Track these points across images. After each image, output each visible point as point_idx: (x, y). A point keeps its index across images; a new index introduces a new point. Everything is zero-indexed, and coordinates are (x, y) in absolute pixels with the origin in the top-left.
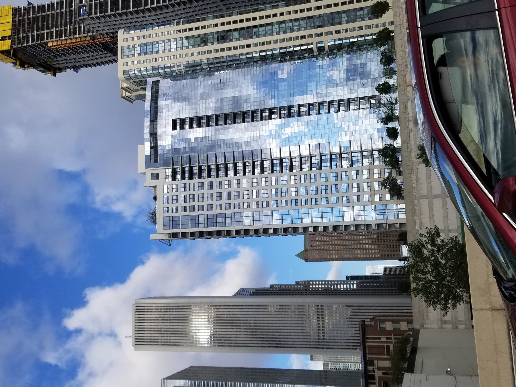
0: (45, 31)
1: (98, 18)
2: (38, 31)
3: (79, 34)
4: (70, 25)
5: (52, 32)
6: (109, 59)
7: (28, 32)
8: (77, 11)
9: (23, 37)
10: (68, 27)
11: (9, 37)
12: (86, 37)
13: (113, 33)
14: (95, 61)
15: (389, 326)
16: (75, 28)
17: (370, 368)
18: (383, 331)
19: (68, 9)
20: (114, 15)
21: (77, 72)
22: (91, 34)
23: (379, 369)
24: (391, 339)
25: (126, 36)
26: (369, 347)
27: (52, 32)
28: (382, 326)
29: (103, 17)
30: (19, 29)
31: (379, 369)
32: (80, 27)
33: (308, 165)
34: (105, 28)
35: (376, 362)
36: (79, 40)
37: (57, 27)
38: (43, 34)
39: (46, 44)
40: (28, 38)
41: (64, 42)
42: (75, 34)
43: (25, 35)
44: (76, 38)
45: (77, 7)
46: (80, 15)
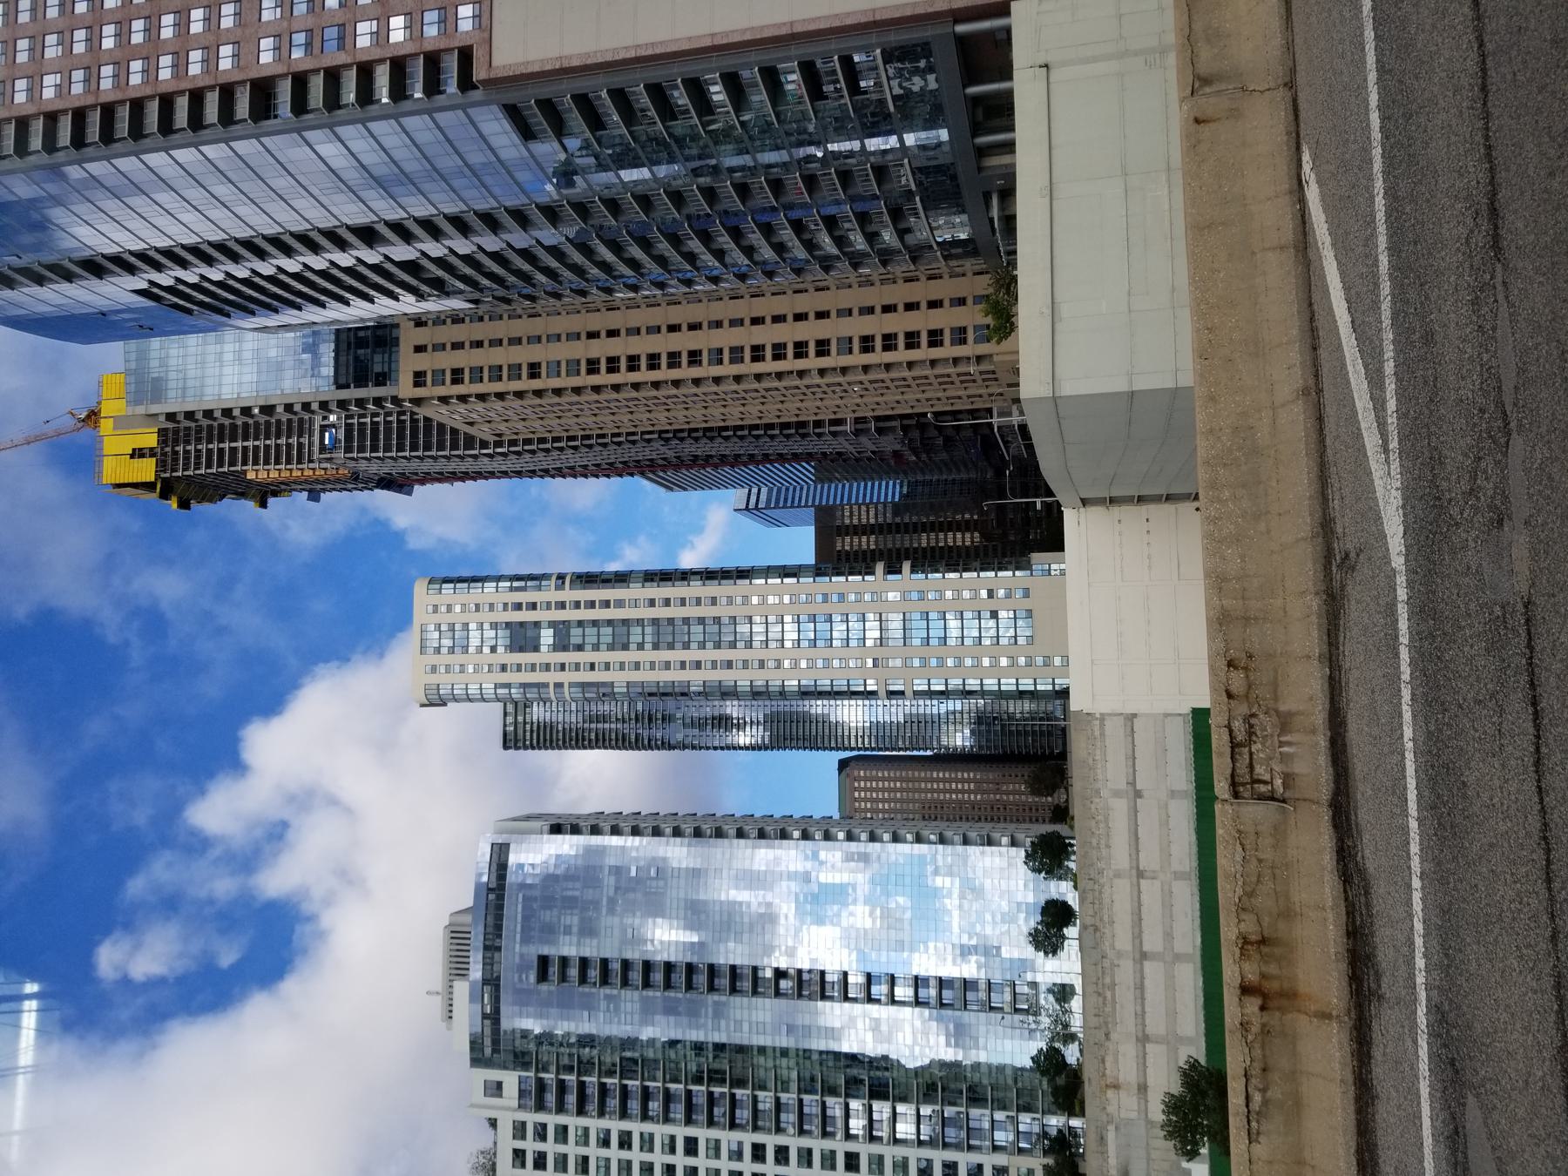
0: (239, 444)
4: (300, 436)
5: (256, 448)
9: (186, 452)
11: (151, 449)
27: (256, 448)
37: (267, 437)
38: (233, 450)
39: (245, 472)
40: (198, 457)
43: (191, 448)
45: (317, 427)
46: (323, 449)
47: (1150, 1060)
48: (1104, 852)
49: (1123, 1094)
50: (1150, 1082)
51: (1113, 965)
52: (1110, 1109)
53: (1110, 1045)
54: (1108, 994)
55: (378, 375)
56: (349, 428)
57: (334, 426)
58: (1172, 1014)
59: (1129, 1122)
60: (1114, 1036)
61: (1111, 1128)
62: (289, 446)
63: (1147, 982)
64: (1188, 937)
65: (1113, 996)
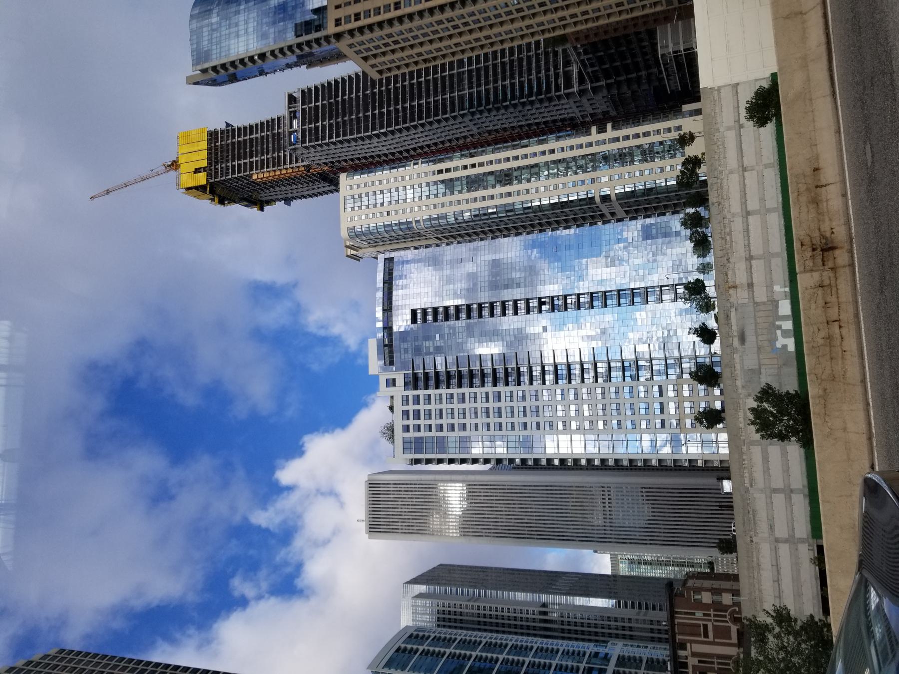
1: (313, 147)
2: (239, 159)
3: (291, 163)
4: (279, 152)
6: (328, 188)
7: (228, 161)
8: (287, 138)
10: (276, 155)
12: (298, 167)
13: (332, 162)
14: (311, 192)
15: (706, 598)
16: (285, 156)
17: (682, 653)
18: (699, 605)
19: (276, 132)
20: (334, 144)
21: (289, 205)
22: (304, 163)
23: (694, 654)
24: (709, 615)
25: (351, 181)
26: (679, 624)
28: (697, 597)
29: (320, 145)
30: (216, 158)
31: (694, 654)
32: (291, 155)
33: (592, 374)
34: (323, 158)
35: (688, 645)
36: (290, 171)
37: (262, 155)
38: (245, 164)
41: (272, 174)
42: (285, 164)
44: (286, 169)
45: (287, 133)
46: (291, 144)
47: (754, 269)
48: (723, 161)
49: (739, 290)
50: (755, 281)
51: (730, 221)
52: (732, 300)
53: (730, 265)
54: (728, 238)
55: (317, 26)
56: (303, 131)
57: (296, 131)
58: (766, 242)
59: (743, 305)
60: (732, 260)
61: (733, 310)
62: (273, 158)
63: (750, 227)
64: (774, 198)
65: (731, 238)
